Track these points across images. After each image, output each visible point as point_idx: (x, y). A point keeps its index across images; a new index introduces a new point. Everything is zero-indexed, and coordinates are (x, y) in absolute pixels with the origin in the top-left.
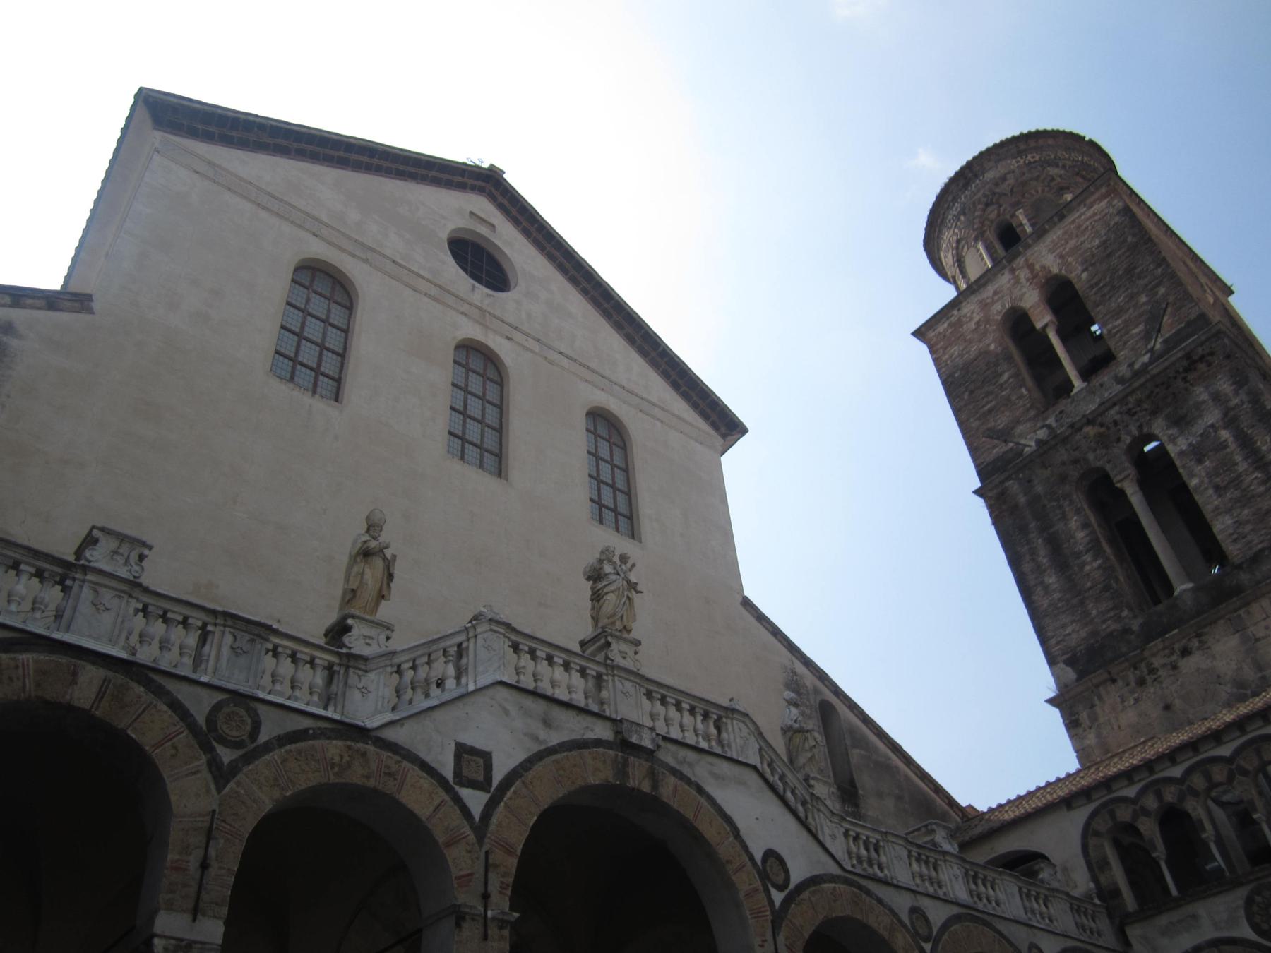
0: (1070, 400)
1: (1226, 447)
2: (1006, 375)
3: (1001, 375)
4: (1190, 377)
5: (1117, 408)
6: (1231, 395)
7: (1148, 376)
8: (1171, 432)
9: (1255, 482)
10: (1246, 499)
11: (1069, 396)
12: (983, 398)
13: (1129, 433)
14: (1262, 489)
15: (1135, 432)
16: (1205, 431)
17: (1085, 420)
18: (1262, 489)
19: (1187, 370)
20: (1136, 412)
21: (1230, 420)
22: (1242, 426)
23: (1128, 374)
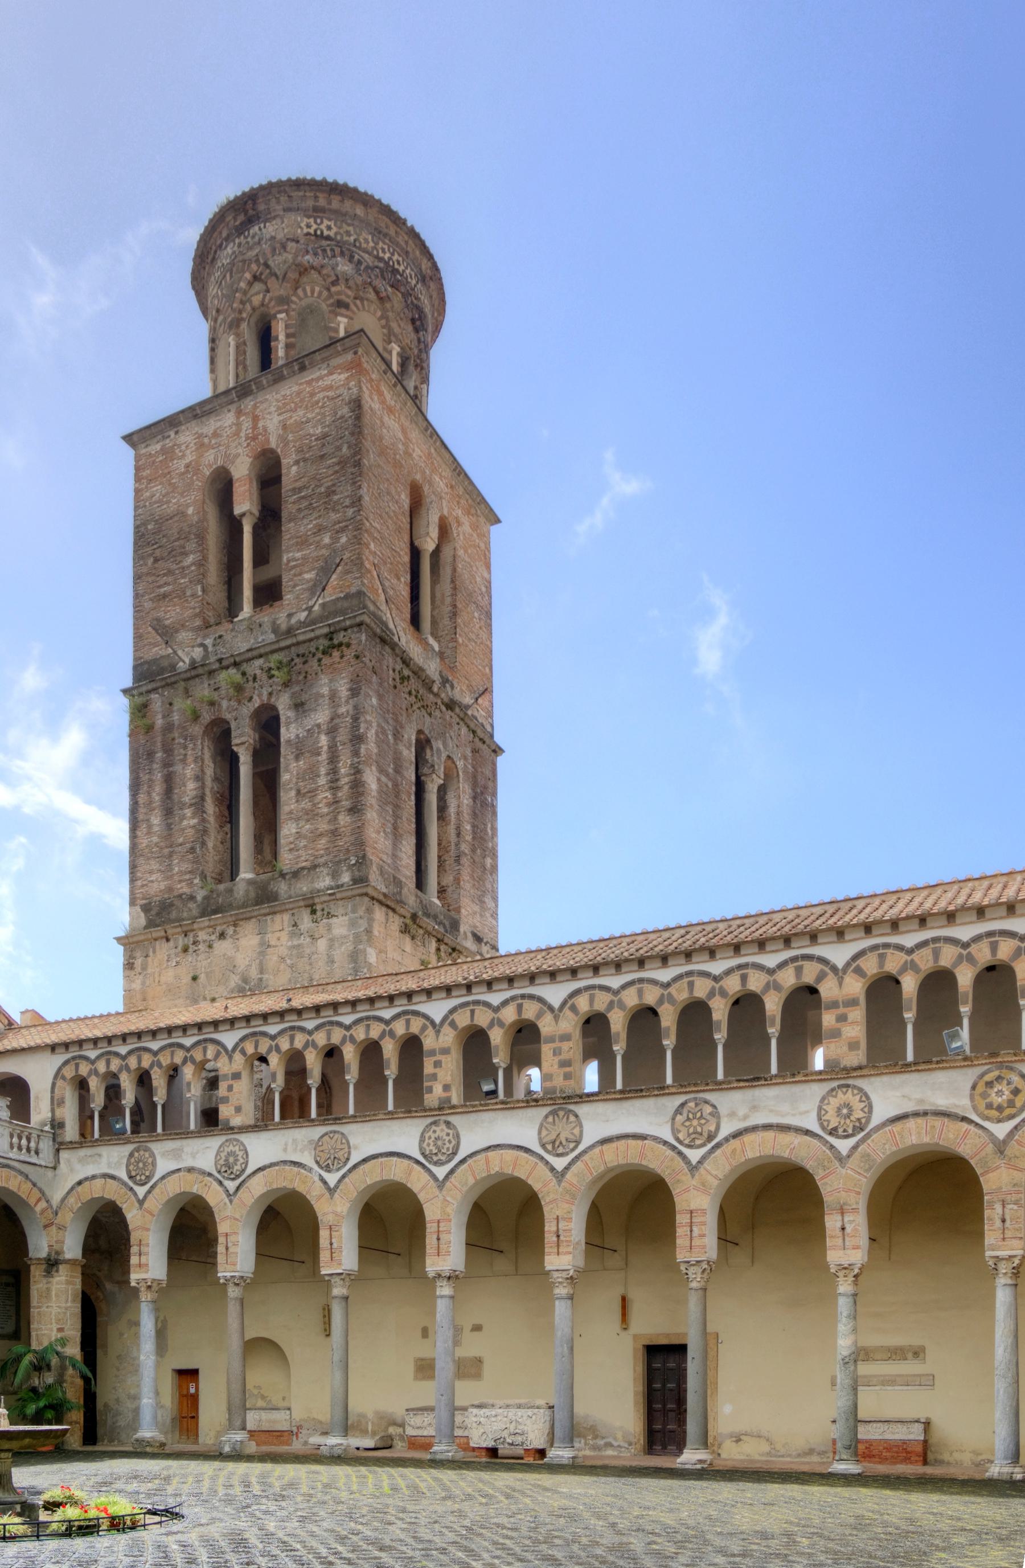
0: (231, 626)
1: (319, 754)
2: (191, 559)
3: (186, 554)
4: (326, 660)
5: (261, 661)
6: (343, 700)
7: (294, 640)
8: (291, 714)
9: (325, 801)
10: (311, 815)
11: (232, 622)
12: (164, 575)
13: (260, 695)
14: (325, 810)
15: (265, 698)
16: (313, 726)
17: (232, 660)
18: (325, 810)
19: (324, 653)
20: (273, 676)
21: (332, 730)
22: (338, 739)
23: (284, 627)
